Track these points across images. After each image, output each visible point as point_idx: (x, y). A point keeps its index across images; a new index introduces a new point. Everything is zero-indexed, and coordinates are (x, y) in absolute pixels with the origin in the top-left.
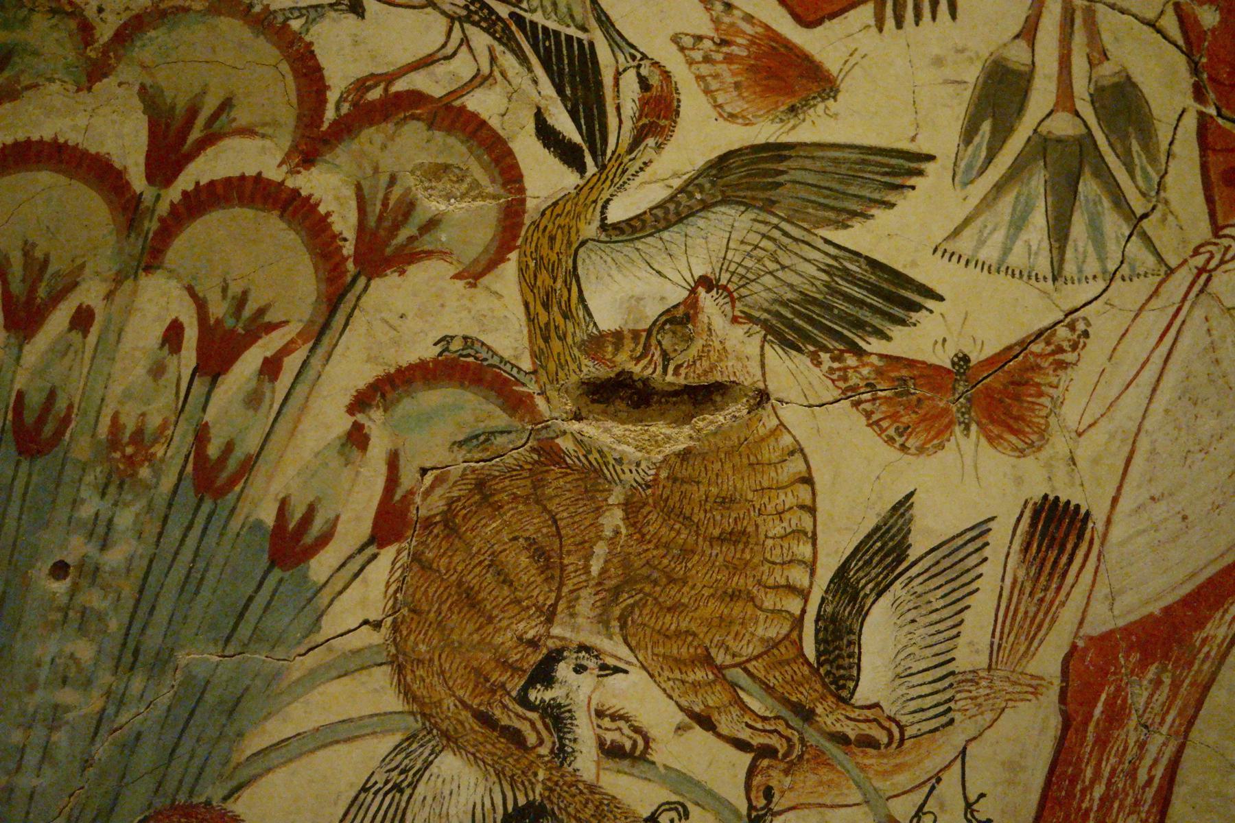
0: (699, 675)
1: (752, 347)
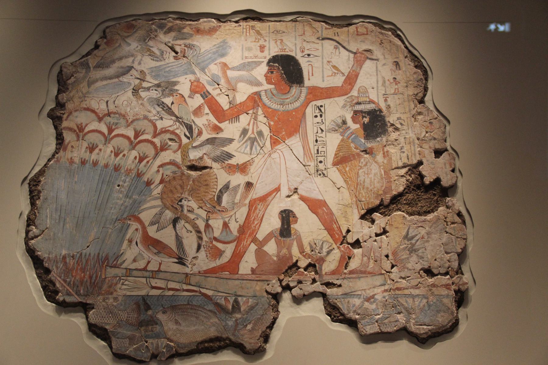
0: (201, 202)
1: (210, 162)
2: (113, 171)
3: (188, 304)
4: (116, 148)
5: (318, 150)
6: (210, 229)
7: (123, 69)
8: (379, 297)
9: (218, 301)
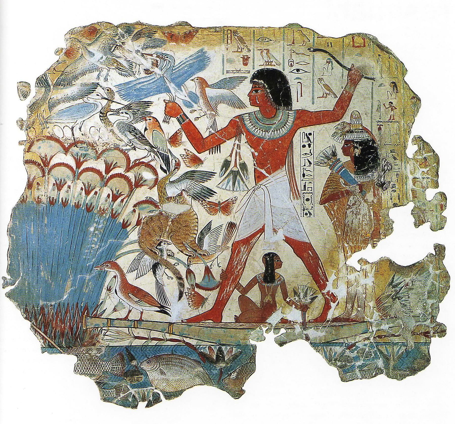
2: (85, 211)
3: (172, 354)
4: (87, 185)
5: (305, 186)
6: (192, 275)
7: (87, 87)
8: (360, 345)
9: (202, 350)
